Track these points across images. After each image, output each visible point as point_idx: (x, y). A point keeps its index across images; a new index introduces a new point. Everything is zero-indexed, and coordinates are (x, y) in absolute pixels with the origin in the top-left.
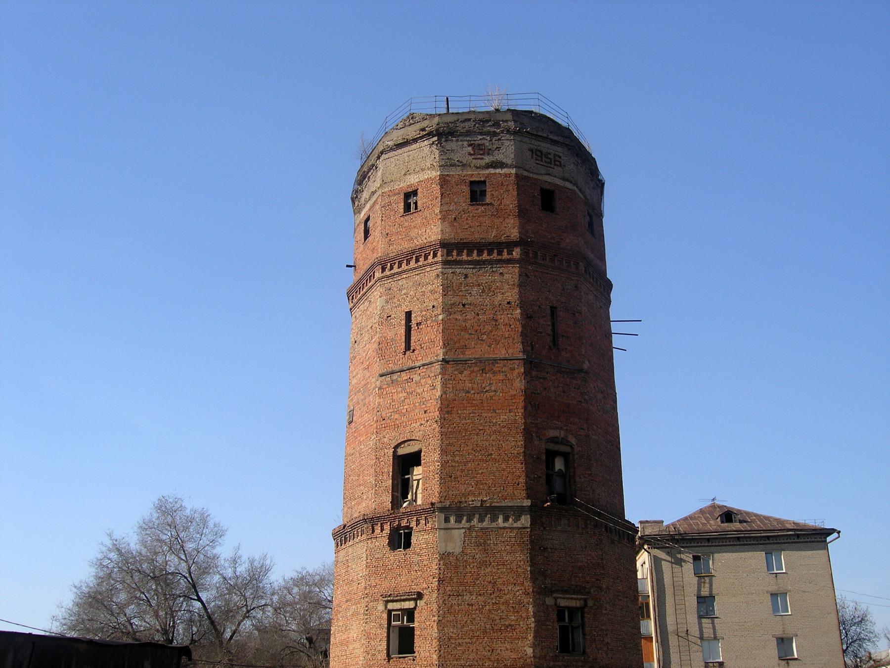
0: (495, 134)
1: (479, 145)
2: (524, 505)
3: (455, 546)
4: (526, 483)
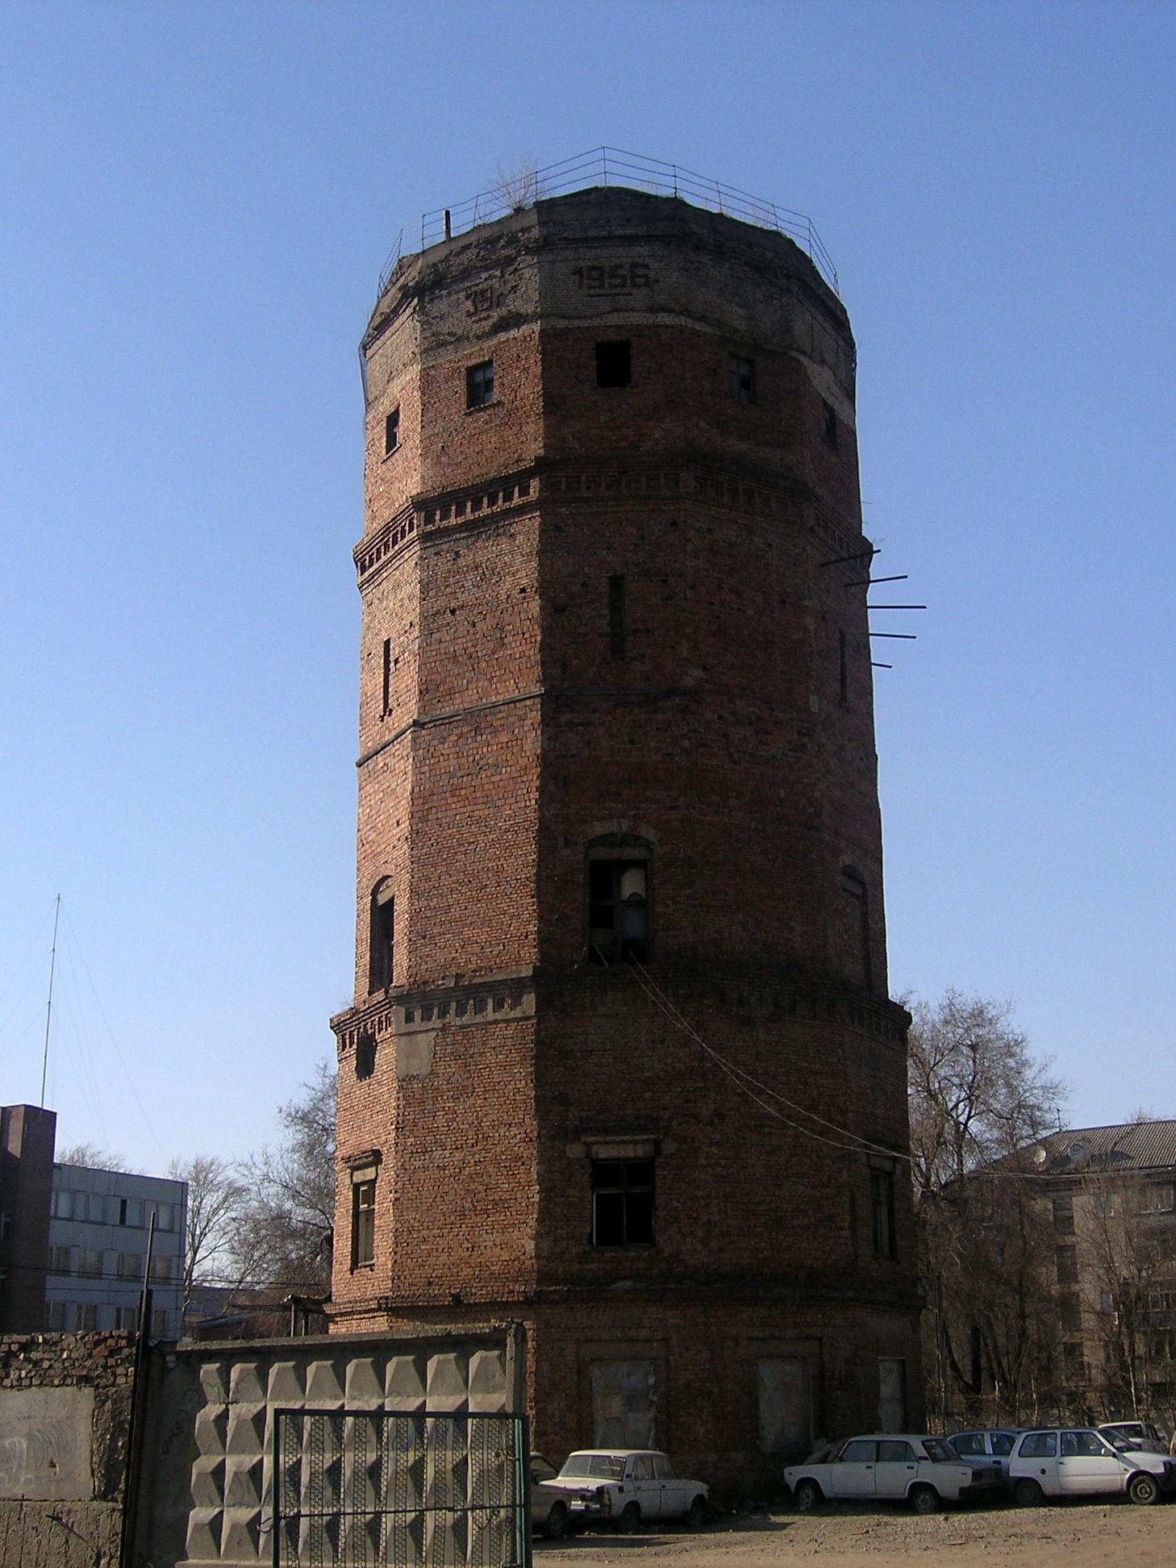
0: (509, 260)
1: (483, 292)
2: (522, 975)
3: (420, 1065)
4: (539, 932)
